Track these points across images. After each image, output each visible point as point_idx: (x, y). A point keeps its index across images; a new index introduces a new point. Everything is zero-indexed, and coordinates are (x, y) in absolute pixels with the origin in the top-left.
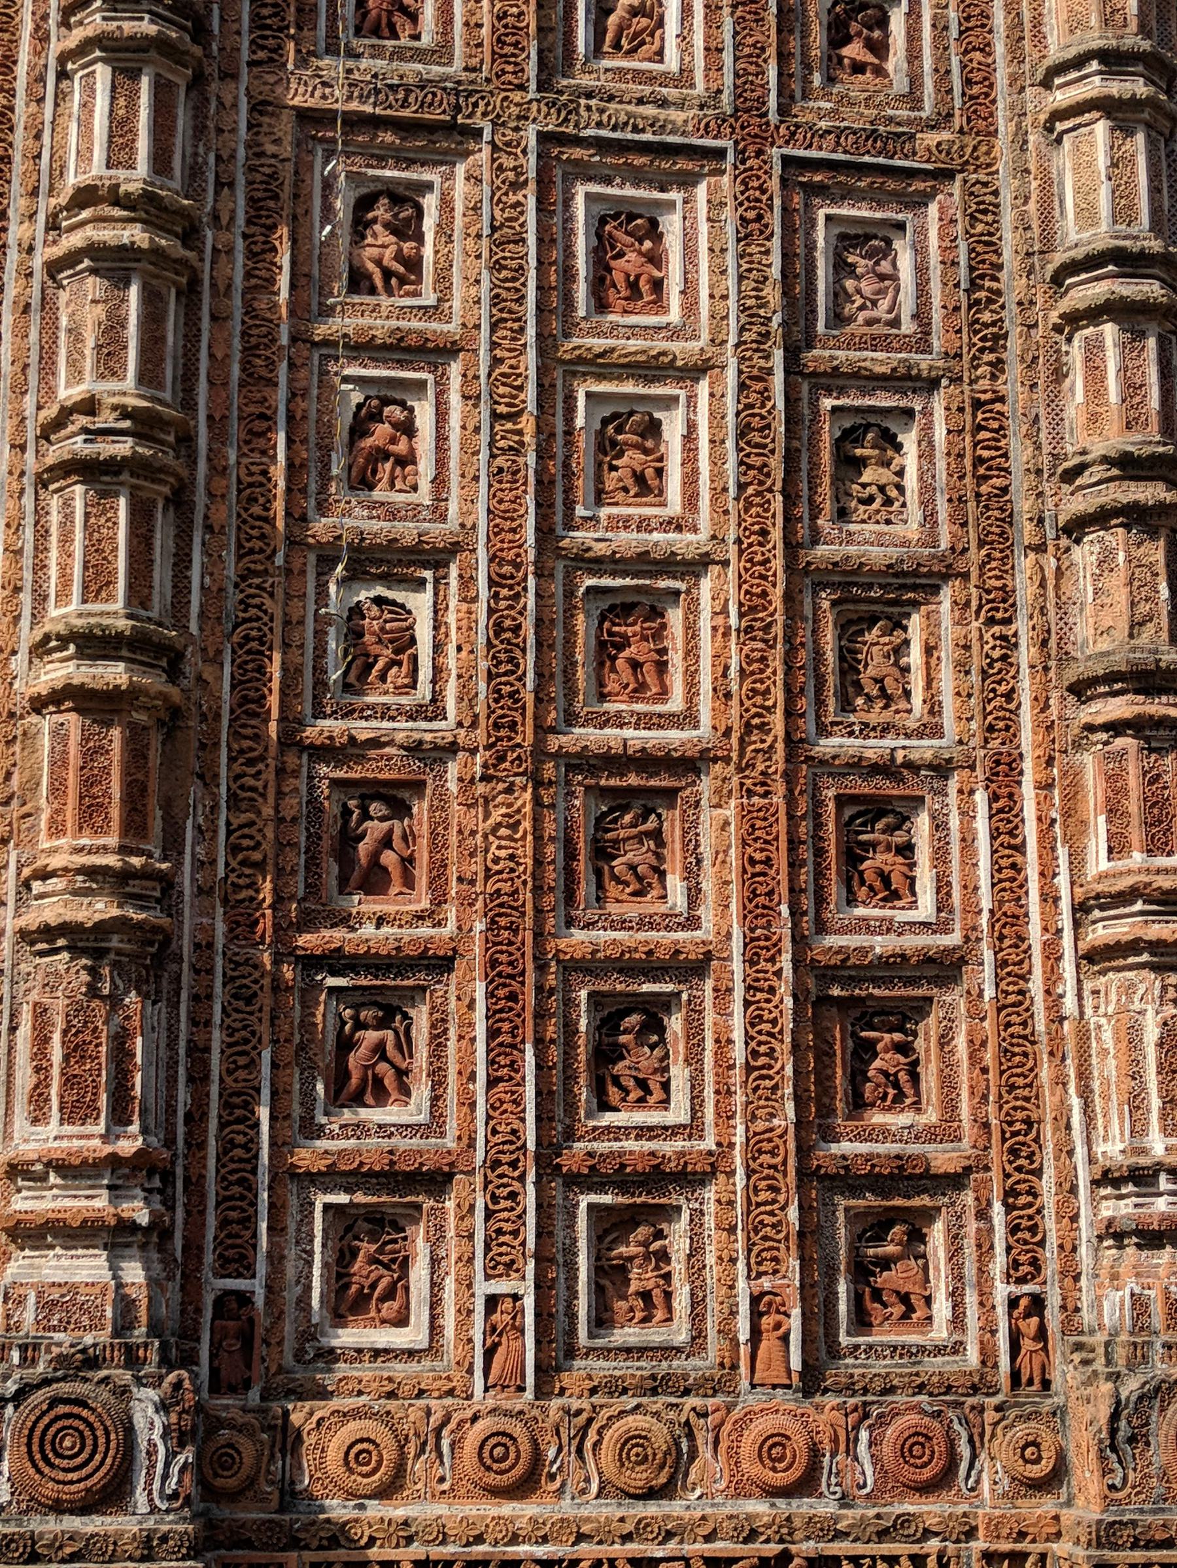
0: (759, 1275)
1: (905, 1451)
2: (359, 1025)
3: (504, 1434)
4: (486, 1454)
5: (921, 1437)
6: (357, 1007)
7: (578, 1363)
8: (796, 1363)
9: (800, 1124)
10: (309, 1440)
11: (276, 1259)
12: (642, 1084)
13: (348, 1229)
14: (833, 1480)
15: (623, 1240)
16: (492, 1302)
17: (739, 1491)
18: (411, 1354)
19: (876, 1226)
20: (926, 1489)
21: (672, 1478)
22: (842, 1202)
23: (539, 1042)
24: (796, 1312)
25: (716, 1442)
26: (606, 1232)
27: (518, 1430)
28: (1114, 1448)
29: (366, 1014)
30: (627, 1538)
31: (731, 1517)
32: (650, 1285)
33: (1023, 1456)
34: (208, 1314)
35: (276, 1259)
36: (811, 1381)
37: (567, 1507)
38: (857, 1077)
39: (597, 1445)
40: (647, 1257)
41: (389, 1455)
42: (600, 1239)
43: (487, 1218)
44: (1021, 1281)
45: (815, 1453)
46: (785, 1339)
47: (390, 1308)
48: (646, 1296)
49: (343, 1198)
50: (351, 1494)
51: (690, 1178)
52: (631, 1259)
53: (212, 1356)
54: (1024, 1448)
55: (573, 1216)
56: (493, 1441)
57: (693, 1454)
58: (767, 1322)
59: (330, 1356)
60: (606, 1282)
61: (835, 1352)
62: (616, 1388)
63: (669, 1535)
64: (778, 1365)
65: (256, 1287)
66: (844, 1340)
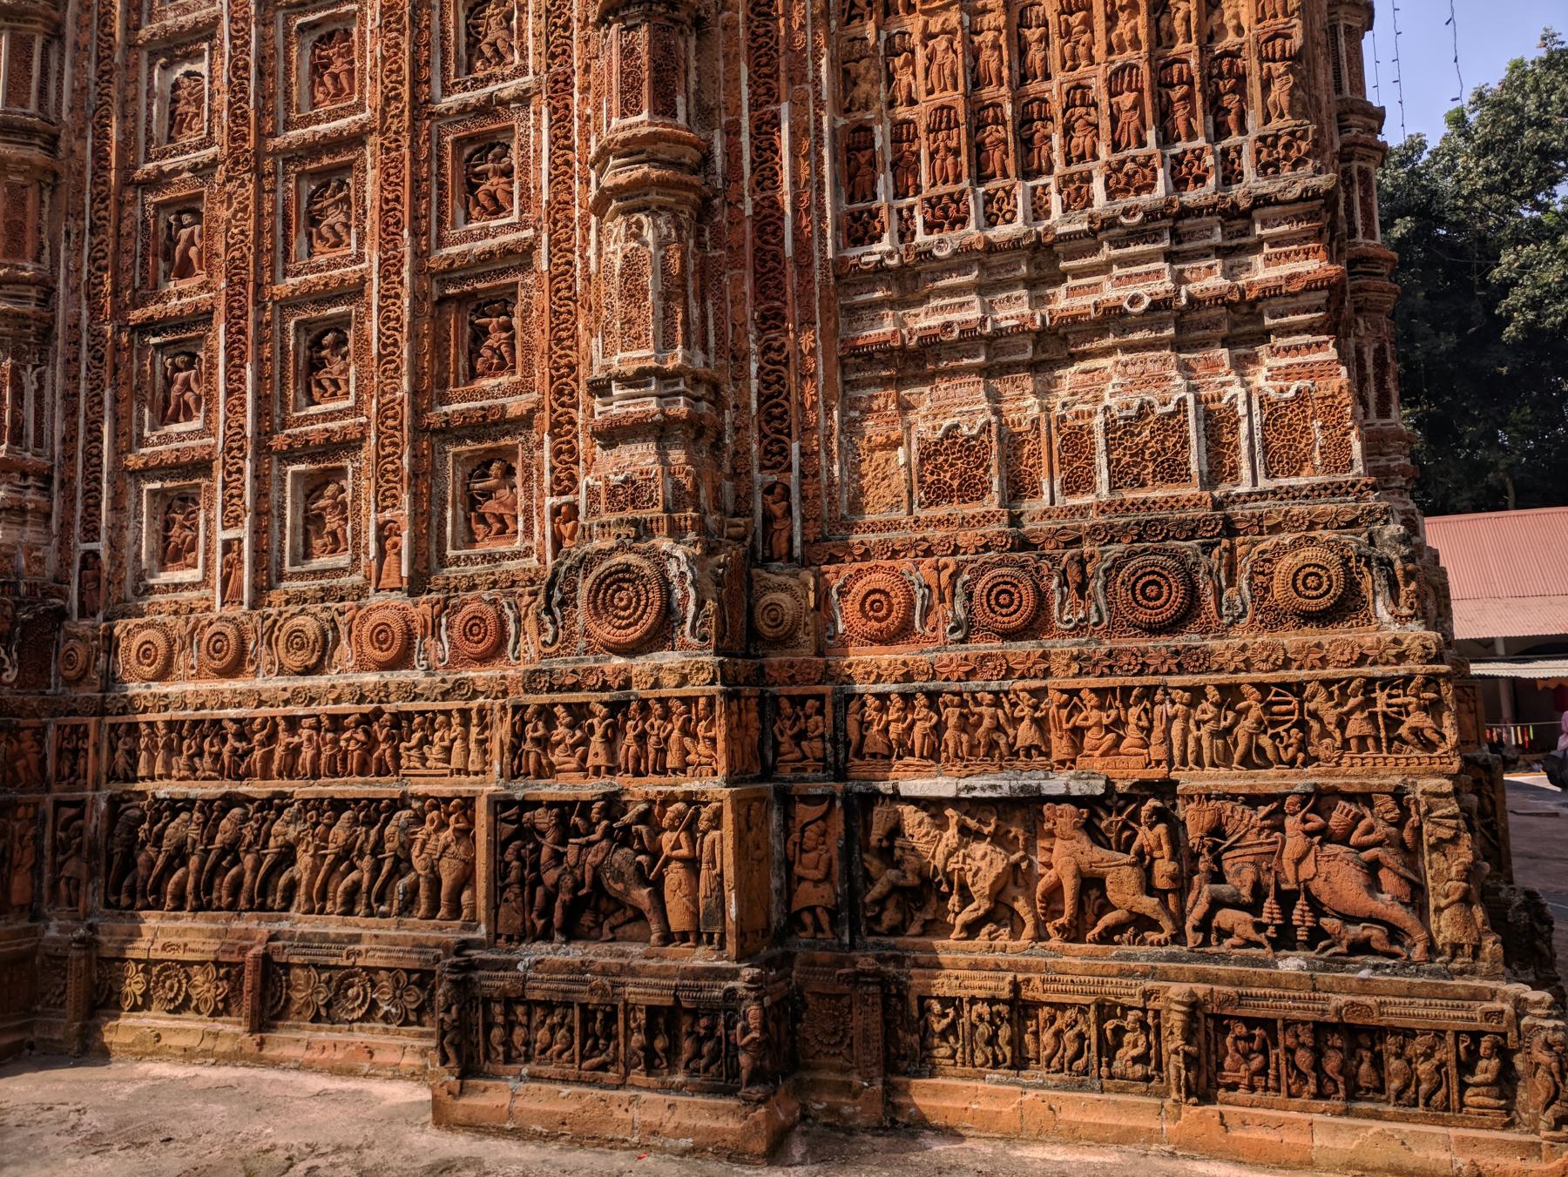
0: (384, 509)
1: (467, 632)
2: (177, 369)
5: (477, 619)
6: (173, 357)
7: (285, 584)
8: (405, 573)
9: (415, 392)
10: (123, 645)
11: (117, 528)
12: (335, 383)
15: (321, 496)
16: (227, 546)
17: (362, 667)
18: (194, 586)
19: (481, 466)
20: (483, 659)
21: (321, 659)
22: (452, 449)
23: (260, 361)
24: (405, 534)
27: (230, 631)
28: (549, 611)
29: (178, 360)
30: (286, 702)
34: (77, 566)
35: (117, 528)
36: (417, 585)
37: (258, 683)
38: (473, 354)
40: (334, 507)
41: (162, 650)
42: (307, 497)
43: (224, 488)
44: (560, 494)
45: (409, 635)
46: (399, 554)
48: (333, 534)
49: (157, 485)
50: (144, 679)
51: (351, 445)
53: (81, 595)
57: (337, 641)
59: (150, 590)
61: (443, 562)
62: (300, 598)
63: (312, 700)
64: (394, 573)
65: (101, 546)
66: (450, 553)
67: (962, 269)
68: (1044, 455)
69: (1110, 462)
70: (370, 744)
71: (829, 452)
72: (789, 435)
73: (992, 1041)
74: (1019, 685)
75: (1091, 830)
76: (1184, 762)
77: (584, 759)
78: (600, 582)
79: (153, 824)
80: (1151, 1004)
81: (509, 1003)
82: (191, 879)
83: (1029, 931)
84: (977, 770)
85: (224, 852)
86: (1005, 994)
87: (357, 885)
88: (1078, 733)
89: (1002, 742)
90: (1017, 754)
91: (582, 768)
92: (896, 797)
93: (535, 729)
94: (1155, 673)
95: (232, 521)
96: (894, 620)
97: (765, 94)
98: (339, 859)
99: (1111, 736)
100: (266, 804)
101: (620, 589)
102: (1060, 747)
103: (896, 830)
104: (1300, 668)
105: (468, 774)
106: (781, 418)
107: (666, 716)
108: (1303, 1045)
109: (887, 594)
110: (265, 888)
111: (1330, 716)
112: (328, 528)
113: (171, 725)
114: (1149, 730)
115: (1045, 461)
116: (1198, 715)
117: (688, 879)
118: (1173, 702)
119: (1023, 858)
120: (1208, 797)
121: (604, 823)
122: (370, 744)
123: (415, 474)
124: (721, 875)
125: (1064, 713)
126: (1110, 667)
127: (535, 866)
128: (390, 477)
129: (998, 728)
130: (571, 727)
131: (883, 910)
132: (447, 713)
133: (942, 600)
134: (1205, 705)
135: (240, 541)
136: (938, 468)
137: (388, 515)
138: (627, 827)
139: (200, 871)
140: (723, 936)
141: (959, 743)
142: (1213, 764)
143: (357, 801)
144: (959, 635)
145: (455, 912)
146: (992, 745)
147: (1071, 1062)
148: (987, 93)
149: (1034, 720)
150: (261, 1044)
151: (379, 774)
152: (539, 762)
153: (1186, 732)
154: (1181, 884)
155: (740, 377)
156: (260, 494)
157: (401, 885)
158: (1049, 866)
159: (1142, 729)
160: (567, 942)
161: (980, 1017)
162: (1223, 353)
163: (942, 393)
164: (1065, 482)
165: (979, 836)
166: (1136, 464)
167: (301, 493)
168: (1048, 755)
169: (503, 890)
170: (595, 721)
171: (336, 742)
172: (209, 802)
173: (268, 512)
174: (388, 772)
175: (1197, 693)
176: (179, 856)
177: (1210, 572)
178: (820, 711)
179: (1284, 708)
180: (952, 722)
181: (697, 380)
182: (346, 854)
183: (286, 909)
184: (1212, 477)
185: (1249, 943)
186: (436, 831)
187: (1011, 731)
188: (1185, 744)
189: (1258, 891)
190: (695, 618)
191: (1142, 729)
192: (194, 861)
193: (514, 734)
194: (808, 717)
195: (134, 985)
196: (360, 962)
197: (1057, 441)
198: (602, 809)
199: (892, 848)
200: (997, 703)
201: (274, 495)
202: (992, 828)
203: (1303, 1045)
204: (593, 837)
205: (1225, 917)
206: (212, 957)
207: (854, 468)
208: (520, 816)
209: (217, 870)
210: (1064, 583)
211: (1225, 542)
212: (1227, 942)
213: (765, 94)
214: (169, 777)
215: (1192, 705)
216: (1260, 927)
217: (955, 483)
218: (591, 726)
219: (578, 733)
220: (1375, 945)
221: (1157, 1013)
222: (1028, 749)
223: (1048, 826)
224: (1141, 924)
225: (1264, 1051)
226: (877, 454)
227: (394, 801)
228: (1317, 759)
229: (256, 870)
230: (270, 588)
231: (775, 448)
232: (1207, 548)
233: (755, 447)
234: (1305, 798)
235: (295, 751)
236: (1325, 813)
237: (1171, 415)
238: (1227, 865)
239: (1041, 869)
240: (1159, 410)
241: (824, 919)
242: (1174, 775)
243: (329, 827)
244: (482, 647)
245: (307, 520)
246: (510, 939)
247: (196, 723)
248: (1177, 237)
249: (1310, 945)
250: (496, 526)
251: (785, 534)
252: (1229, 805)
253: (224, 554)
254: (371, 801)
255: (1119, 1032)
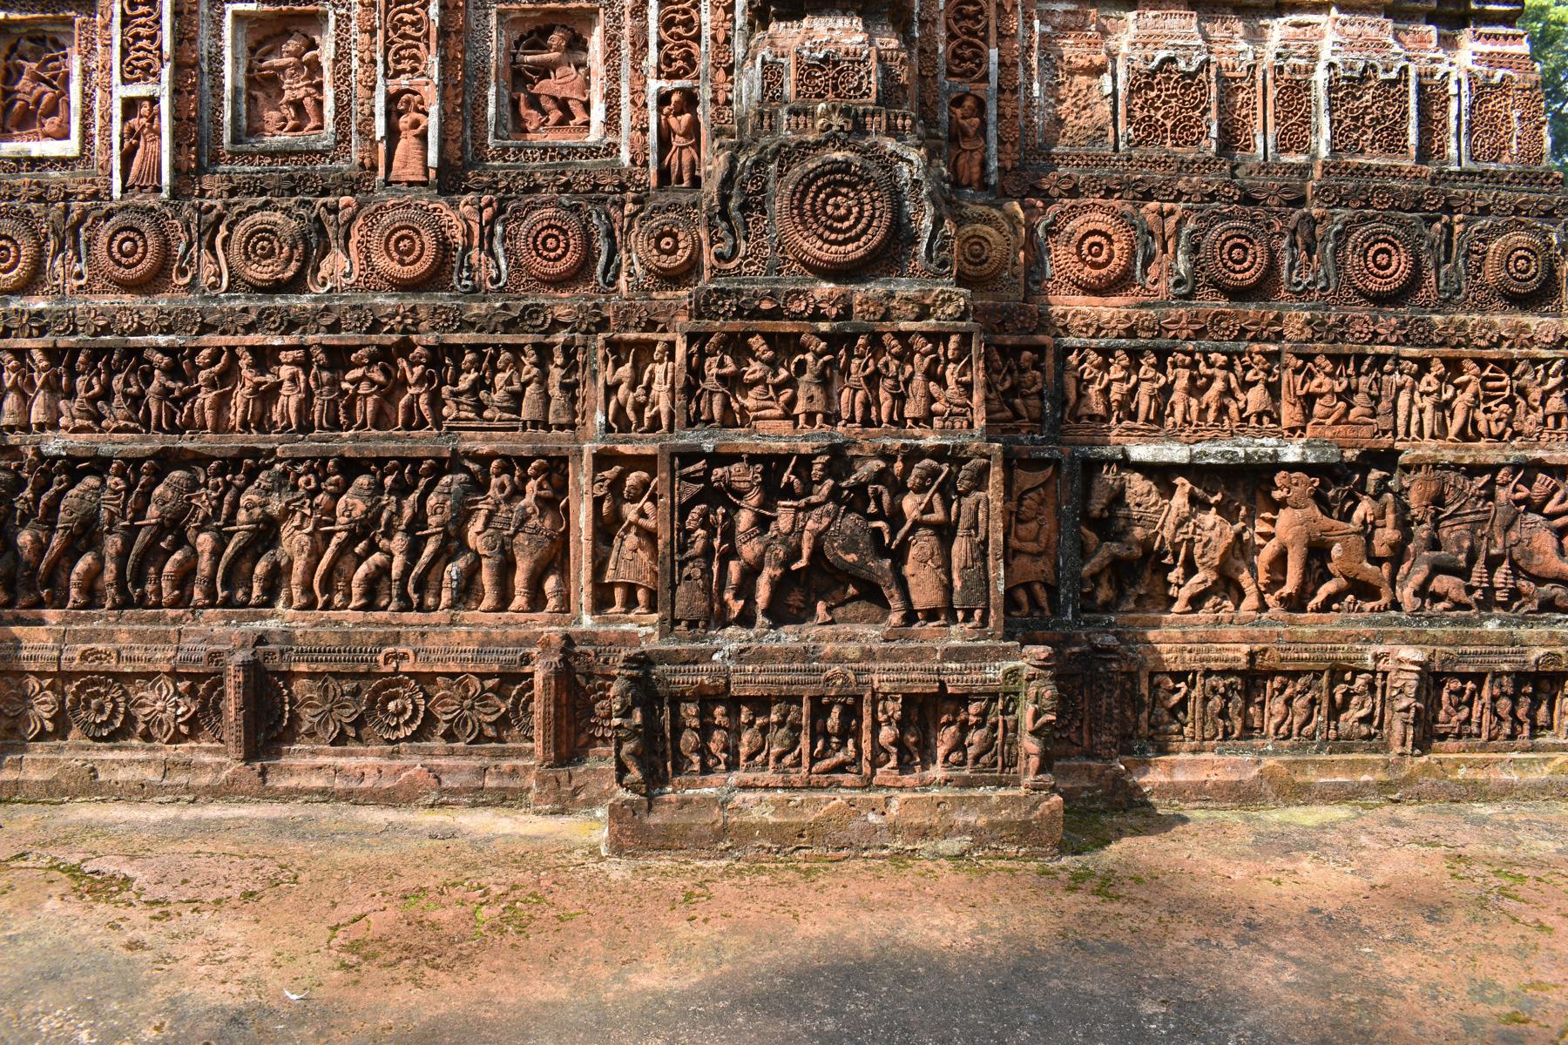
0: (398, 74)
3: (131, 229)
4: (115, 249)
13: (13, 49)
14: (465, 274)
16: (130, 106)
18: (64, 162)
24: (434, 110)
25: (347, 237)
26: (260, 44)
30: (250, 328)
31: (354, 308)
32: (300, 94)
33: (657, 246)
39: (226, 241)
40: (298, 68)
42: (252, 51)
43: (124, 24)
46: (423, 137)
47: (51, 124)
48: (298, 105)
52: (282, 69)
54: (658, 239)
55: (218, 24)
56: (120, 237)
58: (404, 122)
60: (260, 94)
68: (1259, 106)
69: (1332, 122)
70: (391, 388)
71: (1028, 68)
72: (985, 39)
73: (1223, 714)
74: (1256, 347)
75: (1319, 498)
76: (1408, 433)
77: (792, 402)
78: (807, 182)
79: (39, 490)
80: (1381, 665)
81: (706, 699)
82: (110, 566)
83: (1250, 601)
84: (1208, 435)
85: (161, 529)
86: (1243, 664)
87: (384, 570)
88: (1309, 400)
89: (1233, 408)
90: (1247, 419)
91: (788, 414)
92: (1126, 464)
93: (721, 365)
94: (1385, 342)
95: (136, 71)
96: (1117, 265)
98: (353, 539)
99: (1341, 404)
100: (231, 463)
101: (835, 194)
102: (1289, 413)
103: (1118, 498)
104: (1511, 346)
105: (548, 428)
106: (974, 17)
107: (905, 357)
108: (1504, 694)
109: (1108, 237)
110: (236, 575)
111: (1535, 394)
112: (288, 95)
113: (52, 354)
114: (1377, 399)
115: (1259, 112)
116: (1423, 387)
117: (940, 548)
118: (1401, 373)
119: (1244, 529)
120: (1435, 468)
121: (830, 482)
122: (391, 388)
123: (443, 33)
124: (985, 542)
125: (1300, 378)
126: (1343, 334)
127: (729, 534)
128: (409, 30)
129: (1228, 392)
130: (773, 364)
131: (1098, 584)
132: (517, 350)
133: (1165, 251)
134: (1428, 377)
135: (154, 100)
136: (1149, 104)
137: (403, 81)
138: (860, 488)
139: (122, 557)
140: (986, 612)
141: (1188, 408)
142: (1433, 436)
143: (380, 461)
144: (1183, 290)
145: (536, 600)
146: (1223, 410)
147: (1300, 729)
149: (1268, 385)
150: (263, 773)
151: (407, 426)
152: (726, 406)
153: (1412, 402)
154: (1398, 554)
156: (182, 38)
157: (453, 570)
158: (1268, 537)
159: (1372, 397)
160: (775, 627)
161: (1214, 690)
162: (1432, 31)
163: (1150, 22)
164: (1280, 138)
165: (1206, 506)
166: (1356, 128)
167: (242, 46)
168: (1278, 421)
169: (683, 564)
170: (809, 357)
171: (334, 383)
172: (134, 462)
173: (196, 65)
174: (423, 424)
175: (1424, 365)
176: (86, 535)
177: (1432, 247)
178: (1036, 366)
179: (1498, 384)
180: (1182, 383)
182: (364, 530)
183: (269, 603)
184: (1424, 155)
185: (1459, 606)
186: (508, 500)
187: (1240, 395)
188: (1410, 415)
189: (1472, 559)
190: (933, 237)
191: (1372, 397)
192: (112, 544)
193: (690, 370)
194: (1023, 371)
195: (42, 710)
196: (406, 667)
197: (1272, 93)
198: (826, 466)
199: (1113, 517)
200: (1229, 366)
201: (205, 43)
202: (1218, 497)
203: (1504, 694)
204: (814, 499)
205: (1442, 583)
206: (166, 668)
207: (1052, 89)
208: (708, 472)
209: (153, 555)
210: (1293, 244)
211: (1446, 218)
212: (1441, 606)
214: (54, 426)
215: (1418, 377)
216: (1470, 590)
217: (1169, 124)
218: (802, 364)
219: (783, 373)
220: (1558, 603)
221: (1385, 674)
222: (1260, 415)
223: (1277, 495)
224: (1363, 590)
225: (1470, 704)
226: (1078, 79)
227: (440, 460)
228: (1519, 433)
229: (217, 553)
230: (201, 171)
231: (968, 52)
232: (1430, 221)
233: (941, 48)
234: (1516, 468)
235: (266, 396)
236: (1528, 482)
237: (1393, 83)
238: (1445, 533)
239: (1259, 541)
240: (1382, 76)
241: (1042, 595)
242: (1399, 446)
243: (336, 497)
244: (561, 266)
245: (251, 82)
246: (692, 624)
247: (96, 354)
249: (1505, 606)
250: (555, 115)
251: (977, 156)
252: (1452, 474)
253: (125, 119)
254: (404, 461)
255: (1348, 696)
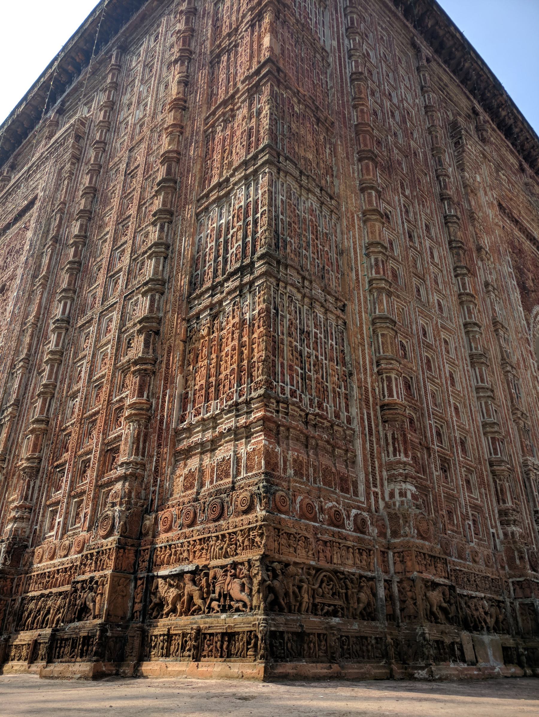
67: (198, 426)
97: (165, 388)
148: (211, 380)
155: (151, 462)
181: (137, 464)
213: (165, 388)
248: (238, 410)
